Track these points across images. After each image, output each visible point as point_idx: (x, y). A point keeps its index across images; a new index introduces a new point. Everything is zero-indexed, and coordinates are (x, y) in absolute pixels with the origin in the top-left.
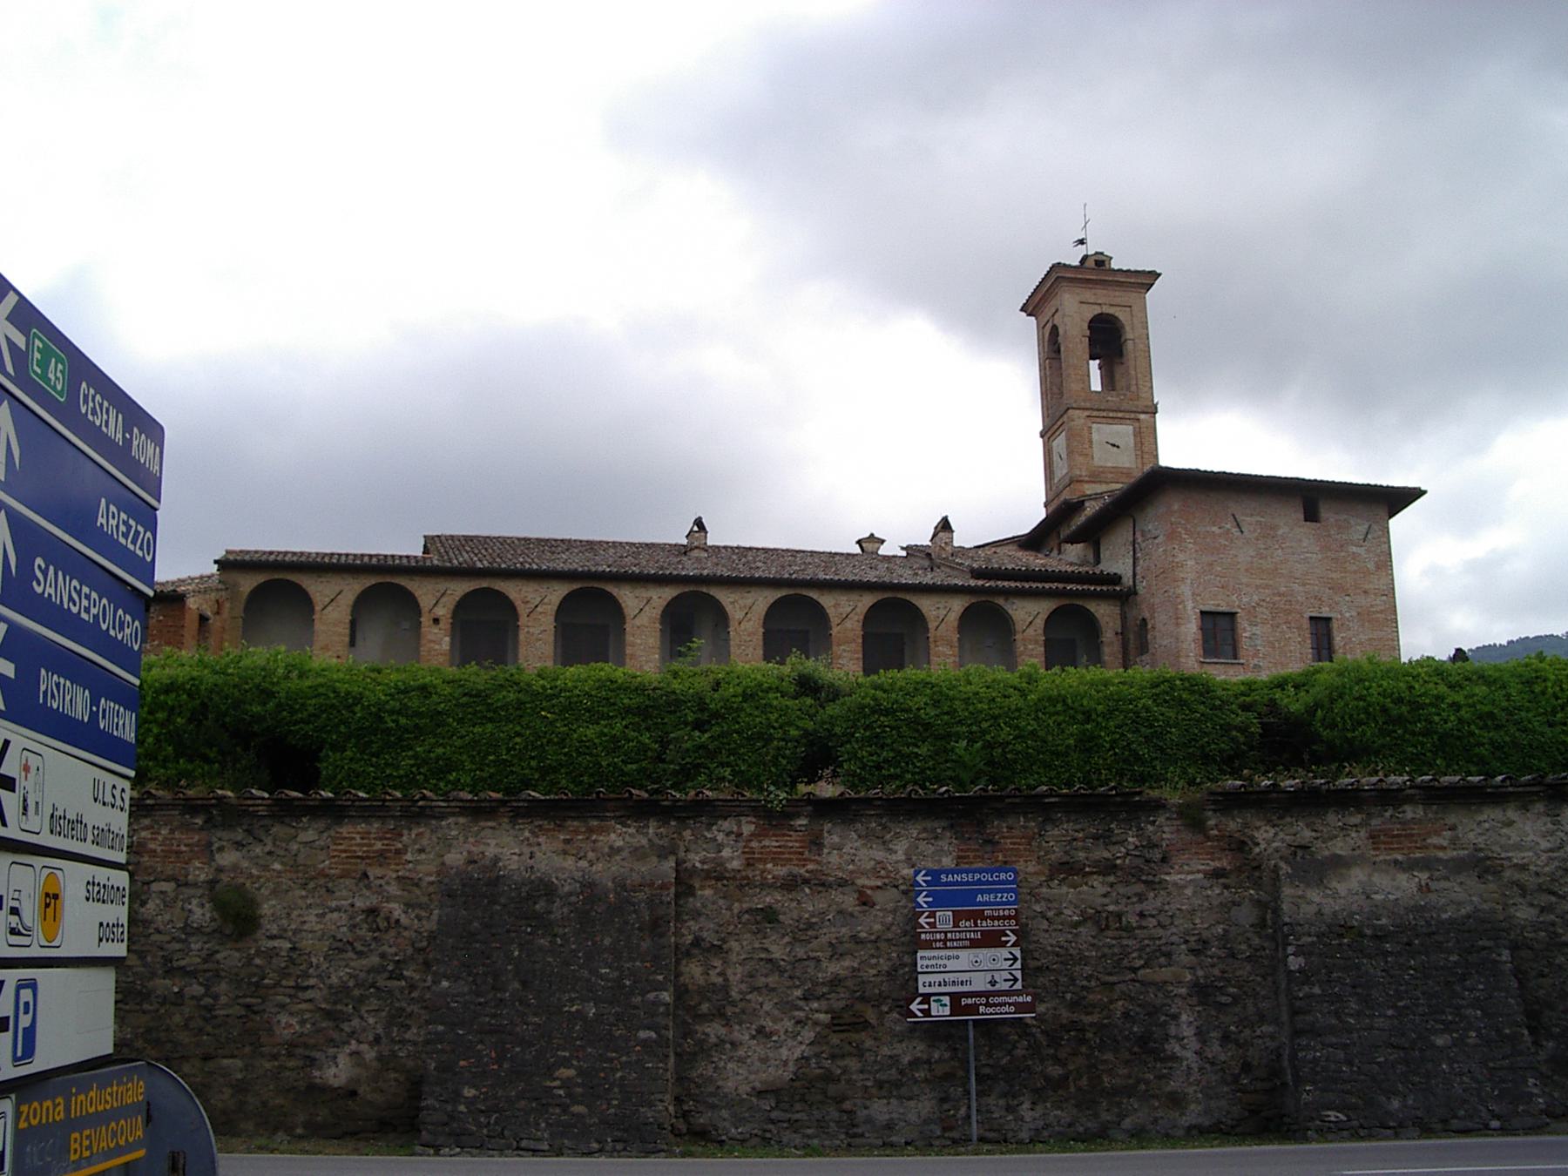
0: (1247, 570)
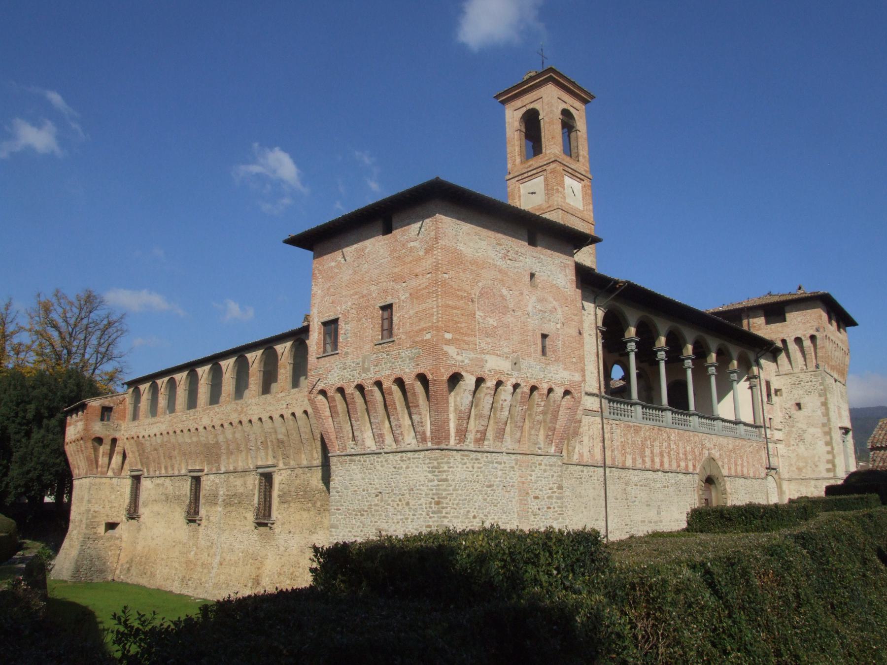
0: (346, 286)
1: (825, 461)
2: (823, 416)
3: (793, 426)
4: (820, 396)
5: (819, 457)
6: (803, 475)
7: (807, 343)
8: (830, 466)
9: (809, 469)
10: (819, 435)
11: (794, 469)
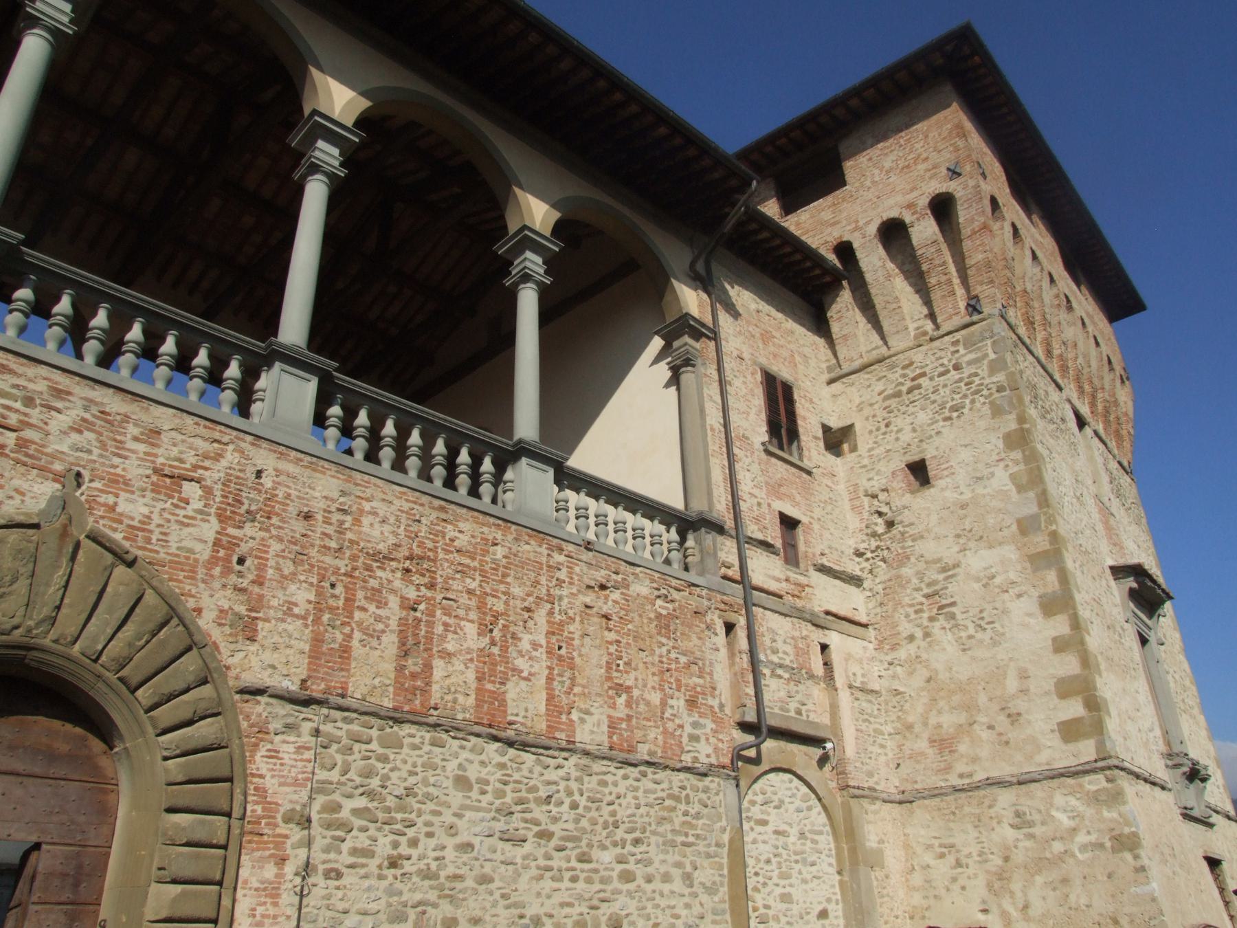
1: (1050, 685)
2: (1020, 489)
3: (904, 559)
4: (997, 411)
5: (1024, 676)
6: (961, 767)
7: (924, 231)
8: (1074, 709)
9: (985, 735)
10: (1012, 576)
11: (922, 745)
